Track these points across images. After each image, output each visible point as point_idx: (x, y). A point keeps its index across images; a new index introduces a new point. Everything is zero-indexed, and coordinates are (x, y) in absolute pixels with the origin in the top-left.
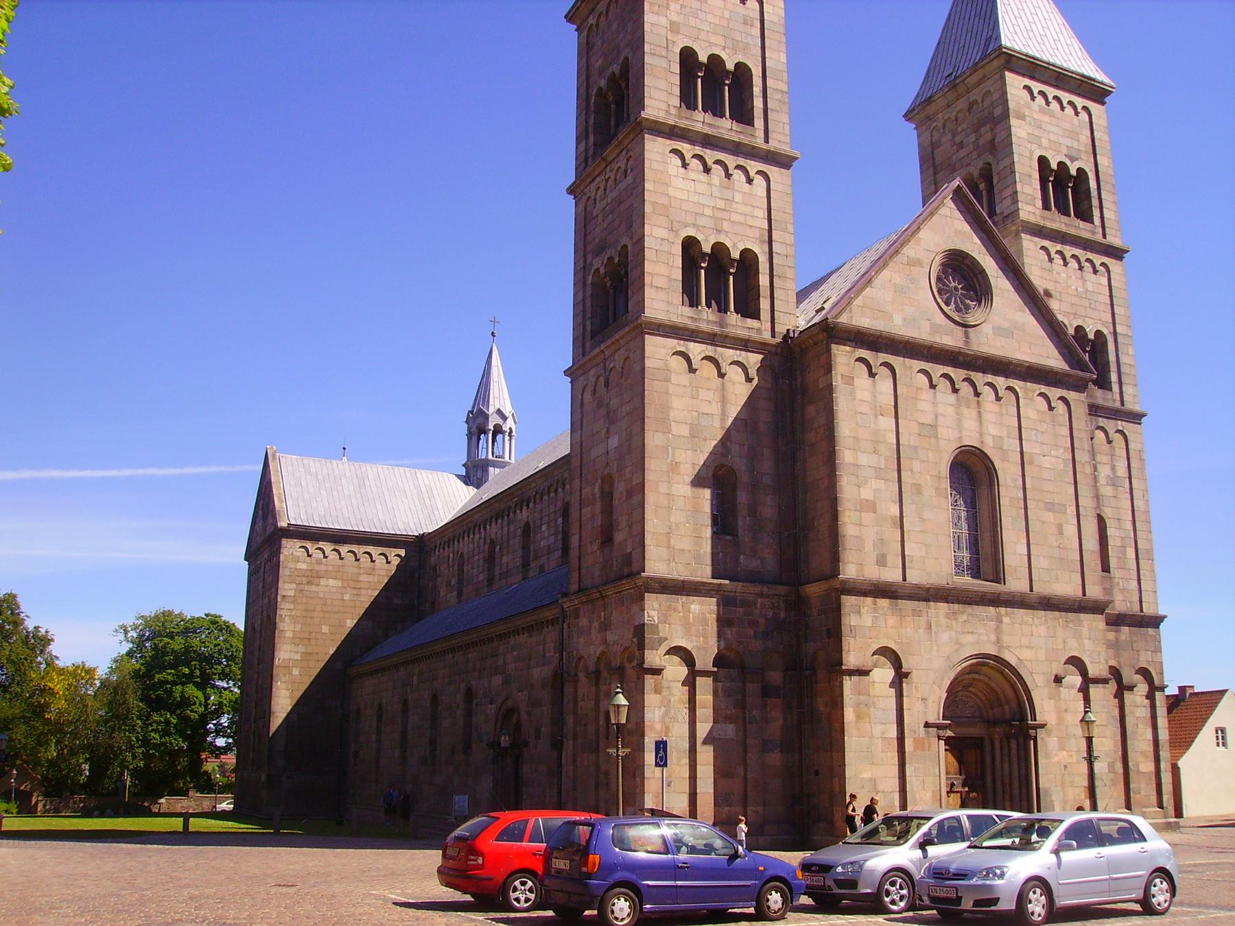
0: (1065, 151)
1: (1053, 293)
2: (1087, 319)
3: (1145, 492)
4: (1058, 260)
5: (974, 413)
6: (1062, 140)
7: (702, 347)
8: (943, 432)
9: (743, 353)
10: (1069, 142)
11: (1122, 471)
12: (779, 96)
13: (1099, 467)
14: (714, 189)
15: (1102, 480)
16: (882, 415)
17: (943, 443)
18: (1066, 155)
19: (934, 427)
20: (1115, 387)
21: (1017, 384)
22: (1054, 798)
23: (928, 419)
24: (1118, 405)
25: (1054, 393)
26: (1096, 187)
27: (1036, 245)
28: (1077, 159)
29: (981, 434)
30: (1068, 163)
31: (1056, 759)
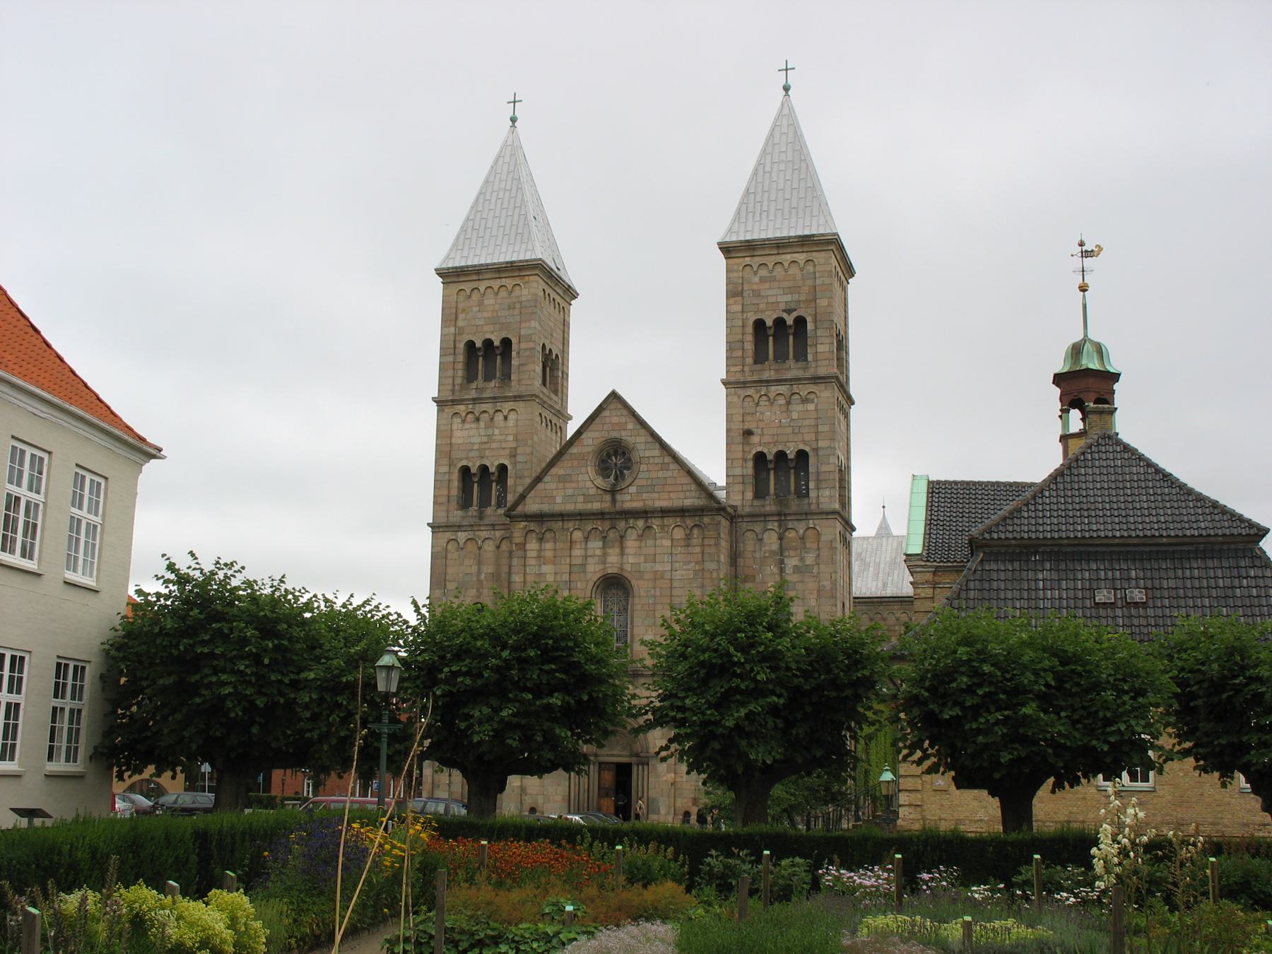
0: (783, 307)
1: (755, 430)
2: (788, 444)
3: (833, 575)
4: (764, 402)
5: (617, 550)
6: (781, 299)
7: (466, 533)
8: (590, 568)
9: (492, 532)
10: (788, 298)
11: (810, 559)
12: (527, 353)
13: (786, 560)
14: (481, 430)
15: (789, 570)
16: (544, 564)
17: (589, 576)
18: (783, 311)
19: (584, 565)
20: (812, 494)
21: (655, 523)
22: (660, 804)
23: (578, 561)
24: (813, 507)
25: (690, 522)
26: (813, 328)
27: (739, 397)
28: (795, 310)
29: (622, 564)
30: (785, 316)
31: (664, 778)
